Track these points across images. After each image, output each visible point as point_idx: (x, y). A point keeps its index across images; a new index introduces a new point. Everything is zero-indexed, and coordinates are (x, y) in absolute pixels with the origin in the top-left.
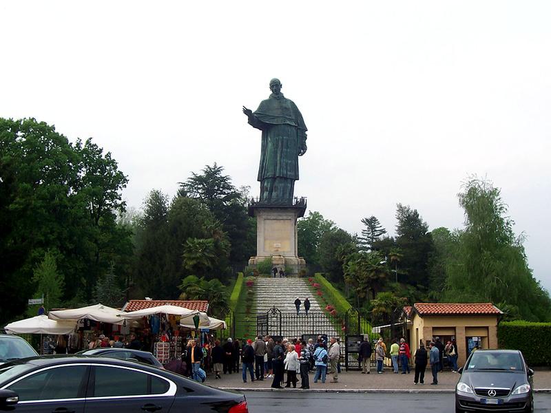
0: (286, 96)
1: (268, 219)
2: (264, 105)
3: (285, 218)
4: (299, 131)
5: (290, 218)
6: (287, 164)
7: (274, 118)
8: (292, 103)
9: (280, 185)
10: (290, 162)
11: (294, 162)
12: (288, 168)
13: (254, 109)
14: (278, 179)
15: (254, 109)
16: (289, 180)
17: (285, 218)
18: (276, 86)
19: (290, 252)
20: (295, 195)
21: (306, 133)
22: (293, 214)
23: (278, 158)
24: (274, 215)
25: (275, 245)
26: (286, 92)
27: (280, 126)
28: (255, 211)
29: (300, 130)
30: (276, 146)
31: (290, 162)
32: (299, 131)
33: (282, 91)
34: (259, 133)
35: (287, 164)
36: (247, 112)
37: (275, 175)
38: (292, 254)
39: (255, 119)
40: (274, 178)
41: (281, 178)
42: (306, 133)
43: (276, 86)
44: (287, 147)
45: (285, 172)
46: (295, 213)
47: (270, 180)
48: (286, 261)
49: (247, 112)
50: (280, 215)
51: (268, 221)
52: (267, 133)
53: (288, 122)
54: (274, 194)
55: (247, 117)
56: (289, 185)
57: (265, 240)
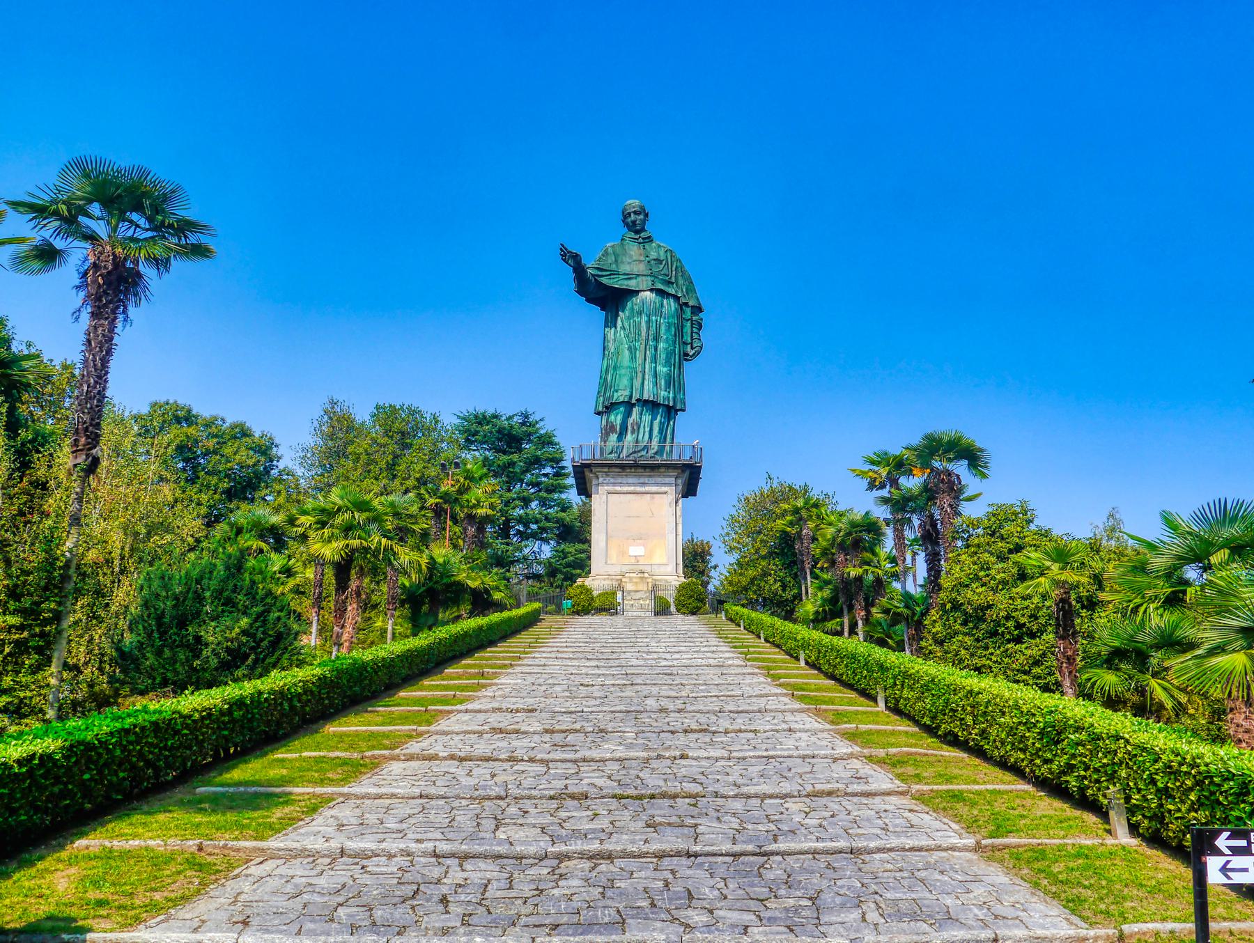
3: (654, 489)
7: (629, 276)
22: (672, 480)
28: (588, 474)
31: (665, 369)
37: (631, 397)
38: (670, 568)
41: (646, 402)
51: (613, 497)
53: (662, 287)
54: (629, 437)
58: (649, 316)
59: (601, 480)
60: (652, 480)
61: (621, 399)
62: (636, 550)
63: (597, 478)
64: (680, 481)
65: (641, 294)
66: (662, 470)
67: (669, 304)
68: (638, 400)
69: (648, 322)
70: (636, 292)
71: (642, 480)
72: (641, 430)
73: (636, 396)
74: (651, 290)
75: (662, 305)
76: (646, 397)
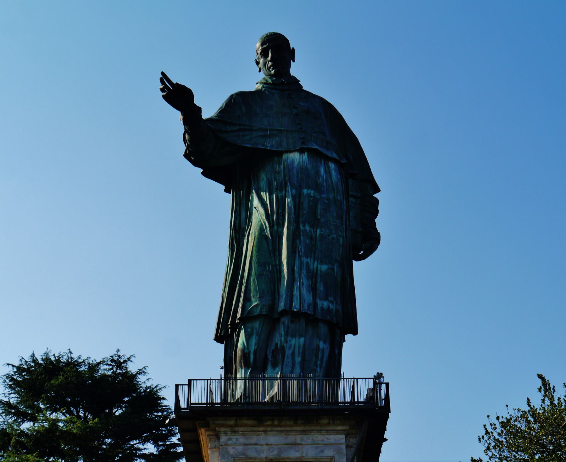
2: (238, 102)
6: (313, 276)
9: (293, 341)
10: (324, 268)
12: (321, 287)
14: (285, 320)
16: (323, 329)
20: (348, 369)
21: (375, 195)
22: (341, 438)
30: (274, 220)
31: (324, 268)
32: (350, 180)
33: (295, 70)
34: (217, 199)
36: (178, 96)
40: (271, 318)
41: (296, 316)
42: (375, 195)
43: (277, 50)
44: (315, 223)
45: (308, 298)
46: (347, 436)
47: (257, 325)
49: (178, 96)
55: (175, 118)
58: (299, 188)
59: (223, 439)
60: (308, 439)
61: (257, 312)
63: (218, 437)
64: (353, 441)
65: (285, 156)
68: (284, 313)
69: (297, 199)
70: (280, 154)
71: (291, 438)
72: (288, 360)
73: (282, 306)
74: (301, 151)
75: (318, 173)
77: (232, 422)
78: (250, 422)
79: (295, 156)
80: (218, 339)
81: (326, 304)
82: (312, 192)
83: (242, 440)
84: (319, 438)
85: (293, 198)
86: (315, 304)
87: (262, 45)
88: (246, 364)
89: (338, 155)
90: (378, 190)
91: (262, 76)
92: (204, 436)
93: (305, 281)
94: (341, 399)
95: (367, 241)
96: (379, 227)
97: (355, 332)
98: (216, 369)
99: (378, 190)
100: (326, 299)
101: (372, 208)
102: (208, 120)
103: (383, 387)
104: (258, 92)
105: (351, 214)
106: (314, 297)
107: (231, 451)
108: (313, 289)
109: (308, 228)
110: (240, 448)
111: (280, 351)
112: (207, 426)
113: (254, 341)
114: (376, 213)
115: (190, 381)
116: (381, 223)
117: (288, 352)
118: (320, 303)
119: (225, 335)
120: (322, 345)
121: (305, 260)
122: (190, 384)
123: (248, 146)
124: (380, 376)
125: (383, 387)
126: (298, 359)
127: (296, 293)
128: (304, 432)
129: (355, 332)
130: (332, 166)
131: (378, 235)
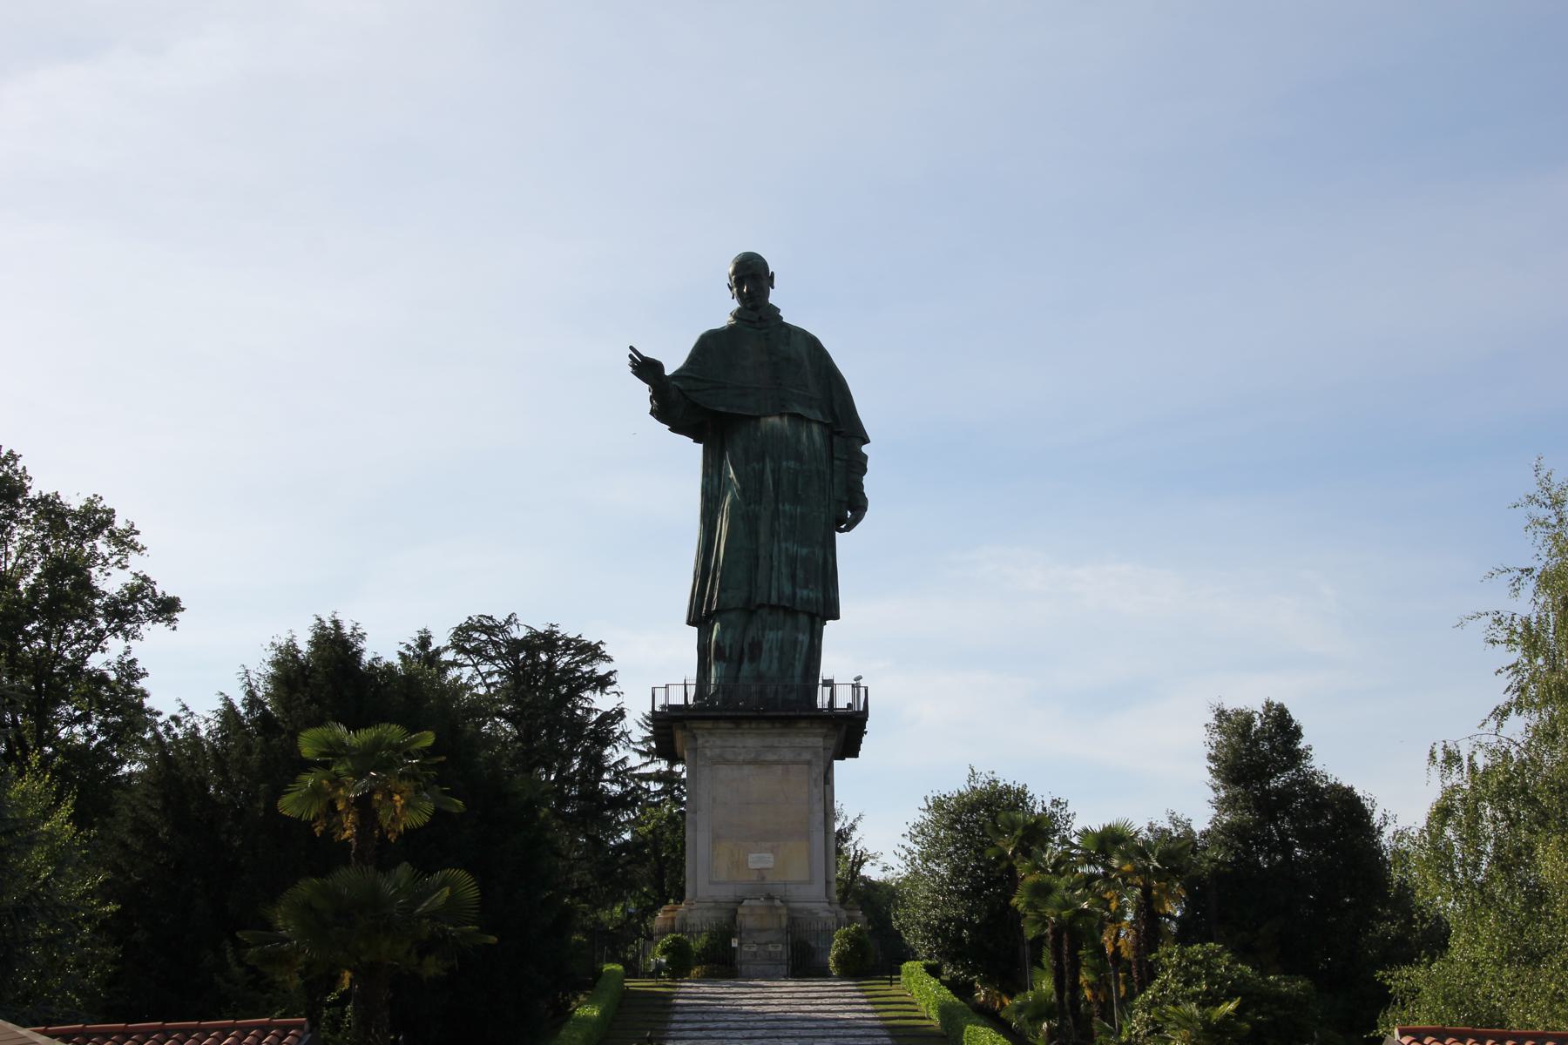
0: (788, 317)
1: (727, 762)
2: (709, 345)
3: (788, 755)
4: (836, 439)
5: (807, 756)
6: (793, 560)
8: (813, 344)
11: (818, 552)
12: (800, 574)
13: (673, 363)
15: (673, 363)
16: (803, 619)
17: (788, 755)
18: (751, 276)
19: (810, 882)
20: (825, 672)
21: (865, 449)
22: (819, 742)
23: (763, 538)
24: (748, 742)
25: (752, 857)
26: (790, 301)
27: (766, 423)
29: (843, 432)
31: (804, 551)
32: (836, 439)
33: (774, 298)
35: (793, 560)
36: (646, 368)
38: (818, 889)
39: (680, 399)
40: (750, 610)
41: (773, 608)
42: (865, 449)
43: (751, 276)
45: (787, 589)
46: (825, 737)
47: (732, 616)
48: (793, 921)
49: (646, 368)
50: (772, 748)
52: (722, 457)
53: (798, 410)
54: (746, 667)
55: (643, 390)
56: (803, 638)
57: (716, 838)
59: (700, 741)
62: (760, 860)
63: (695, 738)
66: (803, 724)
67: (810, 436)
70: (757, 418)
74: (781, 415)
75: (799, 440)
76: (774, 600)
77: (709, 725)
78: (728, 725)
79: (775, 420)
80: (689, 623)
81: (805, 592)
82: (792, 464)
83: (719, 742)
84: (797, 741)
85: (773, 471)
86: (794, 594)
87: (735, 272)
88: (720, 654)
89: (823, 413)
90: (866, 441)
91: (735, 305)
92: (679, 736)
93: (784, 570)
94: (820, 706)
95: (852, 506)
96: (868, 491)
97: (836, 617)
98: (692, 674)
99: (866, 441)
100: (806, 587)
101: (860, 465)
102: (678, 375)
103: (862, 690)
104: (731, 328)
105: (836, 480)
106: (794, 585)
107: (708, 753)
108: (793, 577)
109: (787, 507)
110: (717, 751)
111: (756, 647)
112: (684, 727)
113: (728, 636)
114: (865, 470)
115: (667, 687)
116: (871, 484)
117: (765, 646)
118: (798, 591)
119: (699, 617)
120: (801, 637)
121: (783, 545)
122: (667, 687)
123: (722, 409)
124: (859, 678)
125: (862, 690)
126: (776, 654)
127: (774, 584)
128: (781, 735)
129: (836, 617)
130: (815, 428)
131: (866, 500)
